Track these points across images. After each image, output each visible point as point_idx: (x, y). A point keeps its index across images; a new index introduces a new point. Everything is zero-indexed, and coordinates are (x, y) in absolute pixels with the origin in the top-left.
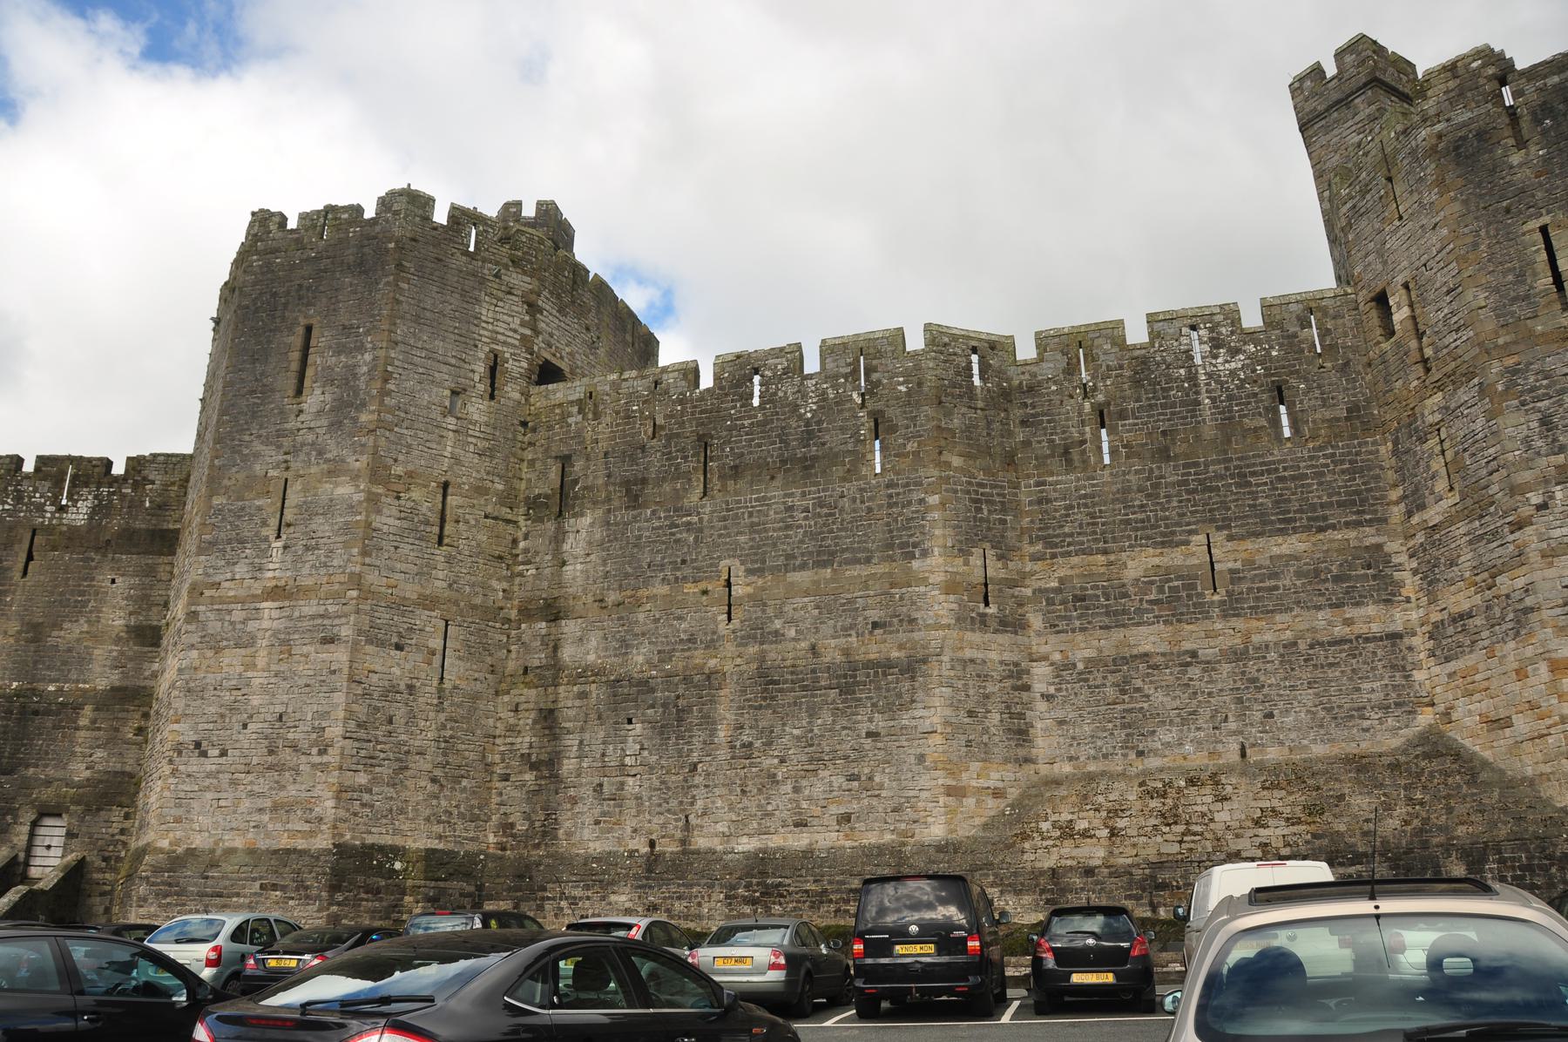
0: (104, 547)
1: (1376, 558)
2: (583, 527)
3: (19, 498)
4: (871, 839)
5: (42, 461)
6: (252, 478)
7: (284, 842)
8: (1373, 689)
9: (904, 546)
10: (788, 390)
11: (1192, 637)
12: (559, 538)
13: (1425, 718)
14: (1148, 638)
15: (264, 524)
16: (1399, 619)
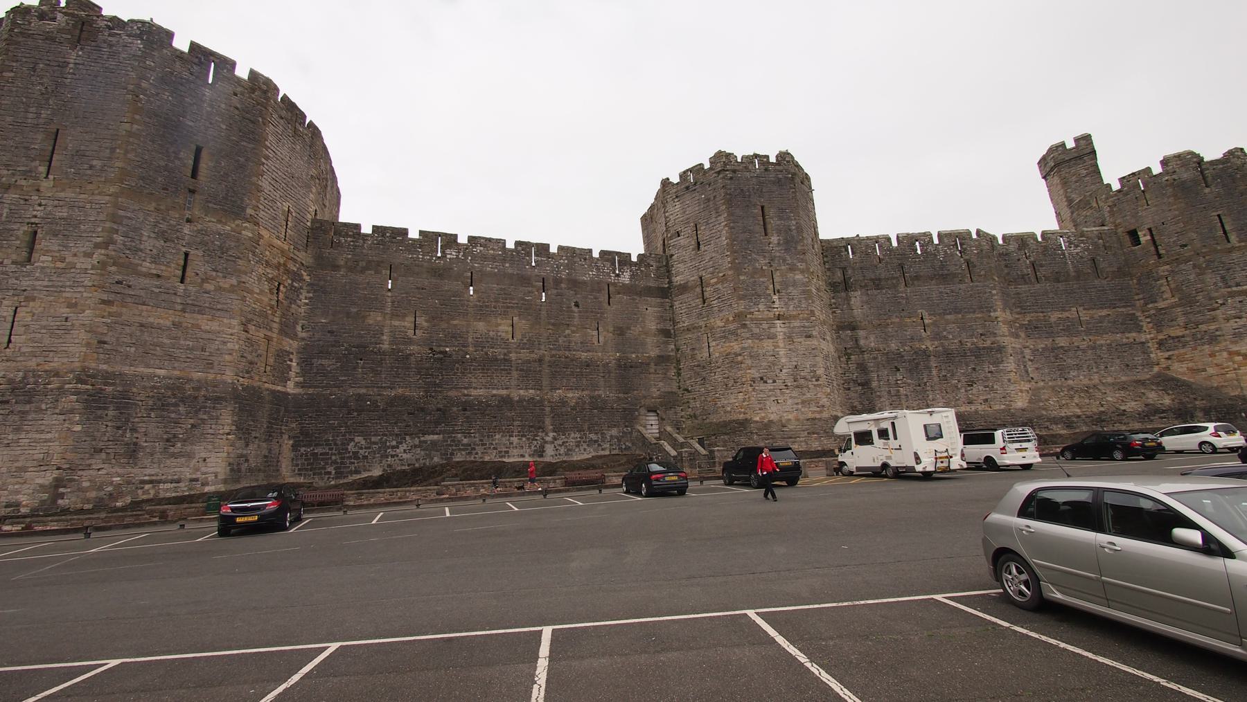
0: (640, 294)
1: (1133, 317)
2: (856, 298)
3: (598, 269)
4: (997, 407)
5: (603, 253)
6: (755, 268)
7: (810, 415)
8: (1139, 359)
9: (990, 309)
10: (930, 248)
11: (1077, 341)
12: (848, 299)
13: (1156, 369)
14: (1062, 341)
15: (767, 288)
16: (1143, 338)
